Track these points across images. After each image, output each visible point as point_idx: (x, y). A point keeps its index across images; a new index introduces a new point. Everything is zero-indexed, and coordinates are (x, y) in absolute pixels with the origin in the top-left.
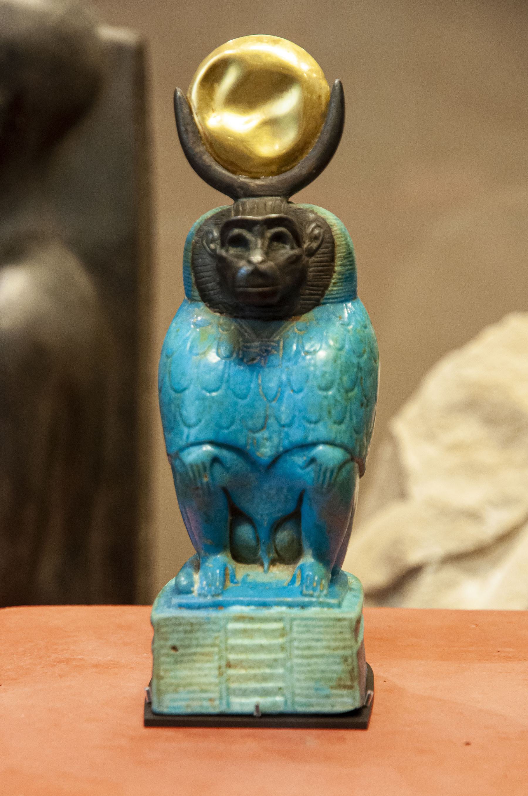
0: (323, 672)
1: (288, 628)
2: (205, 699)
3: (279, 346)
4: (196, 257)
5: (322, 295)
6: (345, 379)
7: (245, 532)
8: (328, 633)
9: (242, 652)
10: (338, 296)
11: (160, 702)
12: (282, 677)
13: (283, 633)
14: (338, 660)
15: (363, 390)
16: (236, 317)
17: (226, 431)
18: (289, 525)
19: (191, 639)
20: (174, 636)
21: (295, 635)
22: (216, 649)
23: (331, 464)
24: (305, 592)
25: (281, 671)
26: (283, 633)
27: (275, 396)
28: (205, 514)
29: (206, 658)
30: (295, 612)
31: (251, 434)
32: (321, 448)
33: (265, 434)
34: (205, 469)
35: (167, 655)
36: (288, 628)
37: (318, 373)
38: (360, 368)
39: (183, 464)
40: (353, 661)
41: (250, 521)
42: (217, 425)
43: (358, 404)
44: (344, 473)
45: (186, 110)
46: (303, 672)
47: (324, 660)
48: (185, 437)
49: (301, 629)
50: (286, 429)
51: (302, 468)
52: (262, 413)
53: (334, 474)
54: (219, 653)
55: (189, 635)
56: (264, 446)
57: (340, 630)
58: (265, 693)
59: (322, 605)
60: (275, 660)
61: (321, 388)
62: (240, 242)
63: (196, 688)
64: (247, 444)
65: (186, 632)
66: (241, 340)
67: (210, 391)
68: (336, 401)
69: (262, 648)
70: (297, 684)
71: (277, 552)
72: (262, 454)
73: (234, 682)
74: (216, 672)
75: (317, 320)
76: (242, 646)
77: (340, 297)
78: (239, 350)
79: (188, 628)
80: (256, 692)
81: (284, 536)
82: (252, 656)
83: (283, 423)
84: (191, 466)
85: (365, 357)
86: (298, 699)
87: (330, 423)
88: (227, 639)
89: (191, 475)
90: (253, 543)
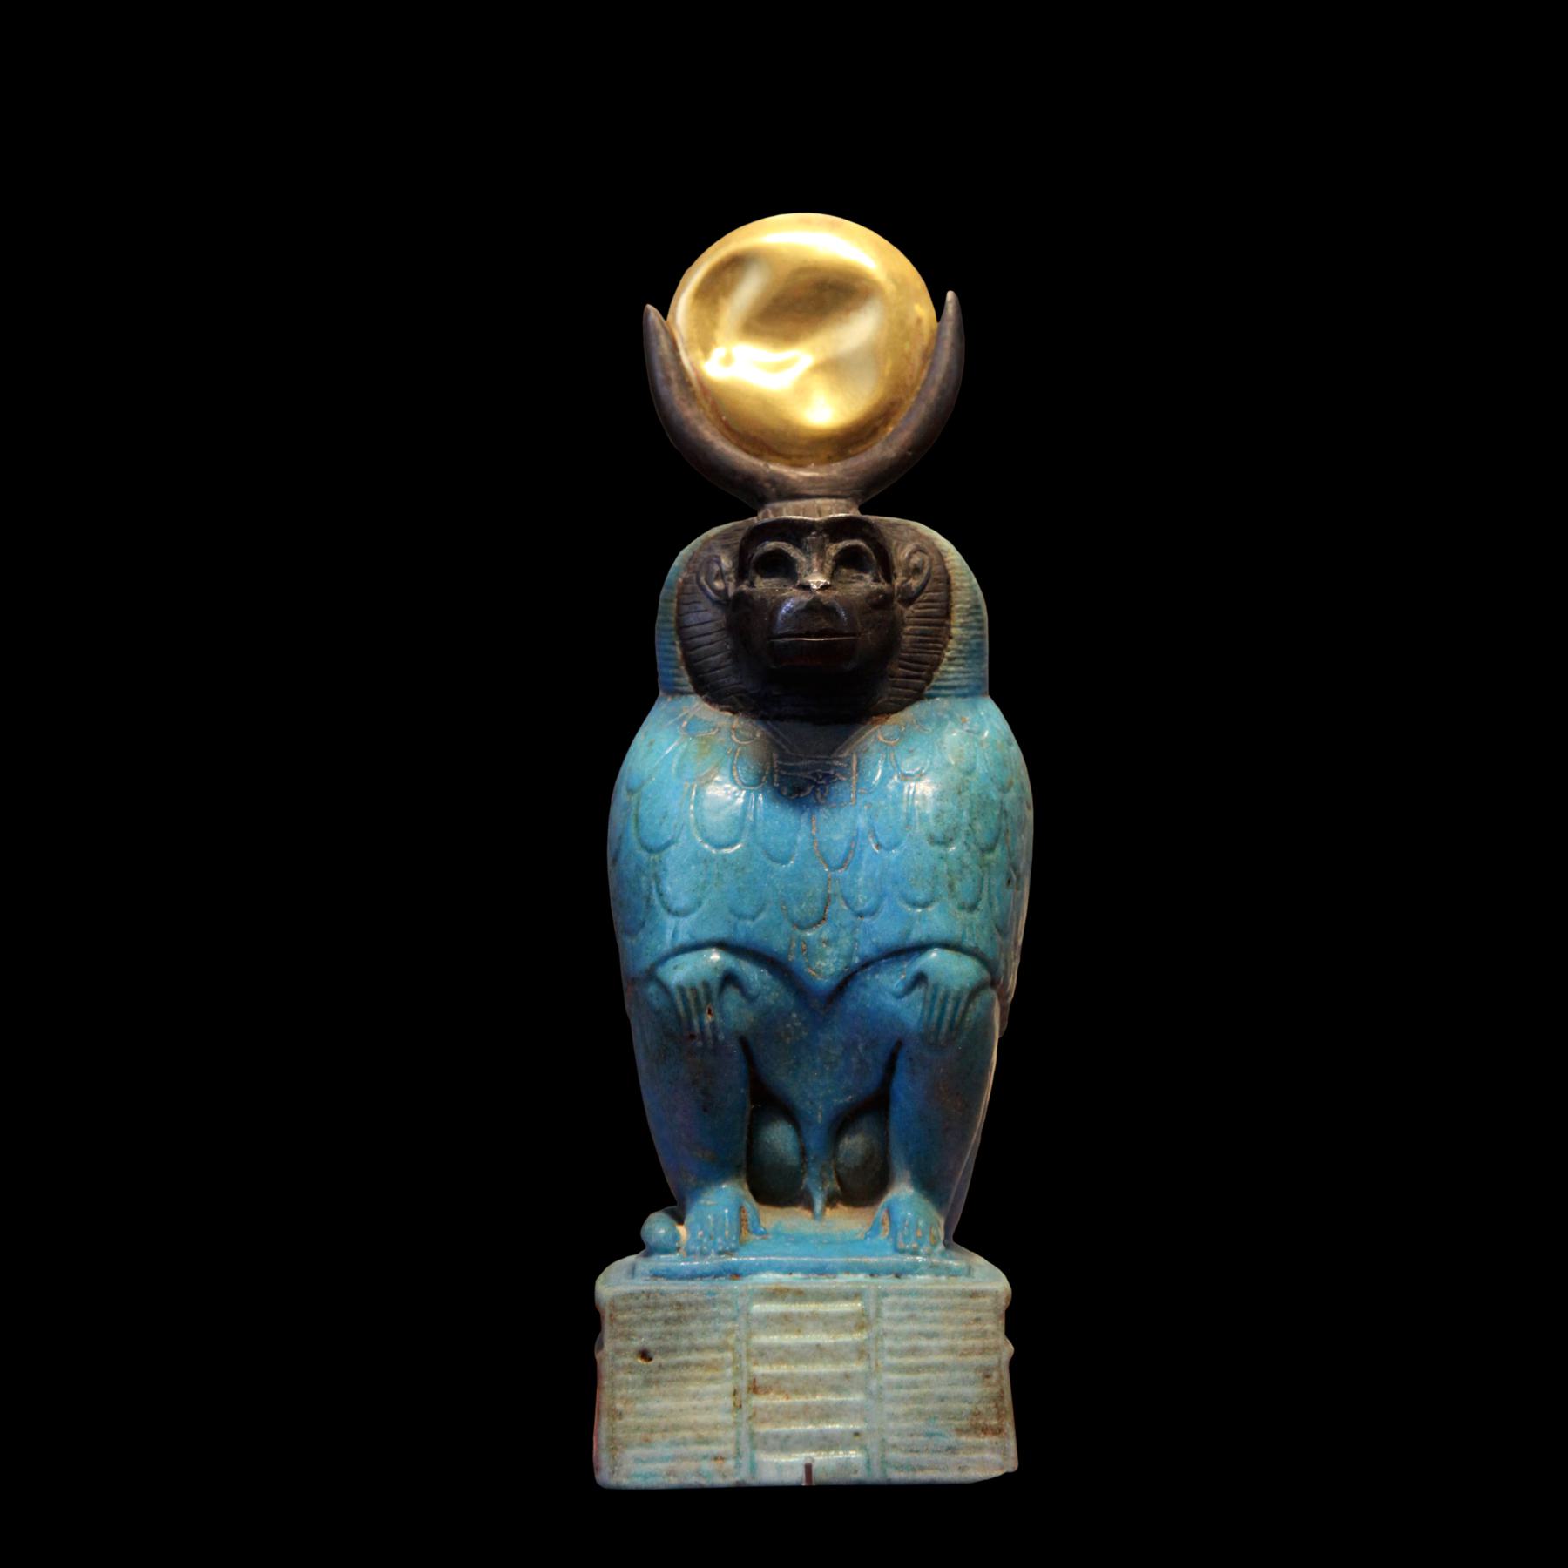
0: (942, 1399)
1: (872, 1311)
2: (705, 1457)
3: (849, 764)
4: (686, 608)
5: (929, 680)
7: (780, 1137)
8: (951, 1322)
9: (781, 1361)
10: (956, 683)
11: (614, 1464)
12: (860, 1411)
13: (861, 1322)
14: (972, 1375)
15: (1010, 855)
16: (763, 718)
17: (749, 923)
18: (865, 1123)
19: (677, 1335)
20: (645, 1329)
21: (887, 1326)
22: (729, 1355)
23: (955, 987)
24: (901, 1245)
25: (857, 1398)
26: (861, 1322)
27: (845, 860)
28: (705, 1092)
29: (709, 1374)
30: (885, 1282)
31: (798, 932)
32: (934, 955)
33: (825, 932)
34: (708, 997)
35: (630, 1369)
36: (872, 1311)
37: (929, 811)
38: (1004, 813)
39: (664, 987)
40: (1001, 1376)
41: (790, 1114)
42: (732, 911)
43: (1002, 878)
44: (977, 1007)
45: (664, 345)
46: (903, 1400)
47: (944, 1376)
48: (668, 937)
49: (898, 1313)
50: (866, 920)
51: (899, 996)
52: (819, 891)
53: (962, 1007)
54: (734, 1362)
55: (674, 1329)
56: (823, 957)
57: (975, 1315)
58: (828, 1443)
59: (934, 1269)
60: (847, 1376)
61: (933, 840)
62: (780, 566)
63: (688, 1434)
64: (789, 951)
65: (667, 1321)
66: (775, 756)
67: (719, 847)
68: (964, 866)
69: (820, 1351)
70: (891, 1425)
71: (840, 1180)
72: (818, 972)
73: (764, 1421)
74: (729, 1402)
75: (920, 721)
76: (781, 1347)
77: (960, 687)
78: (772, 772)
79: (671, 1313)
80: (807, 1442)
81: (854, 1144)
82: (803, 1369)
83: (858, 909)
84: (681, 989)
85: (1012, 794)
86: (893, 1455)
87: (952, 905)
88: (750, 1334)
89: (681, 1009)
90: (793, 1159)
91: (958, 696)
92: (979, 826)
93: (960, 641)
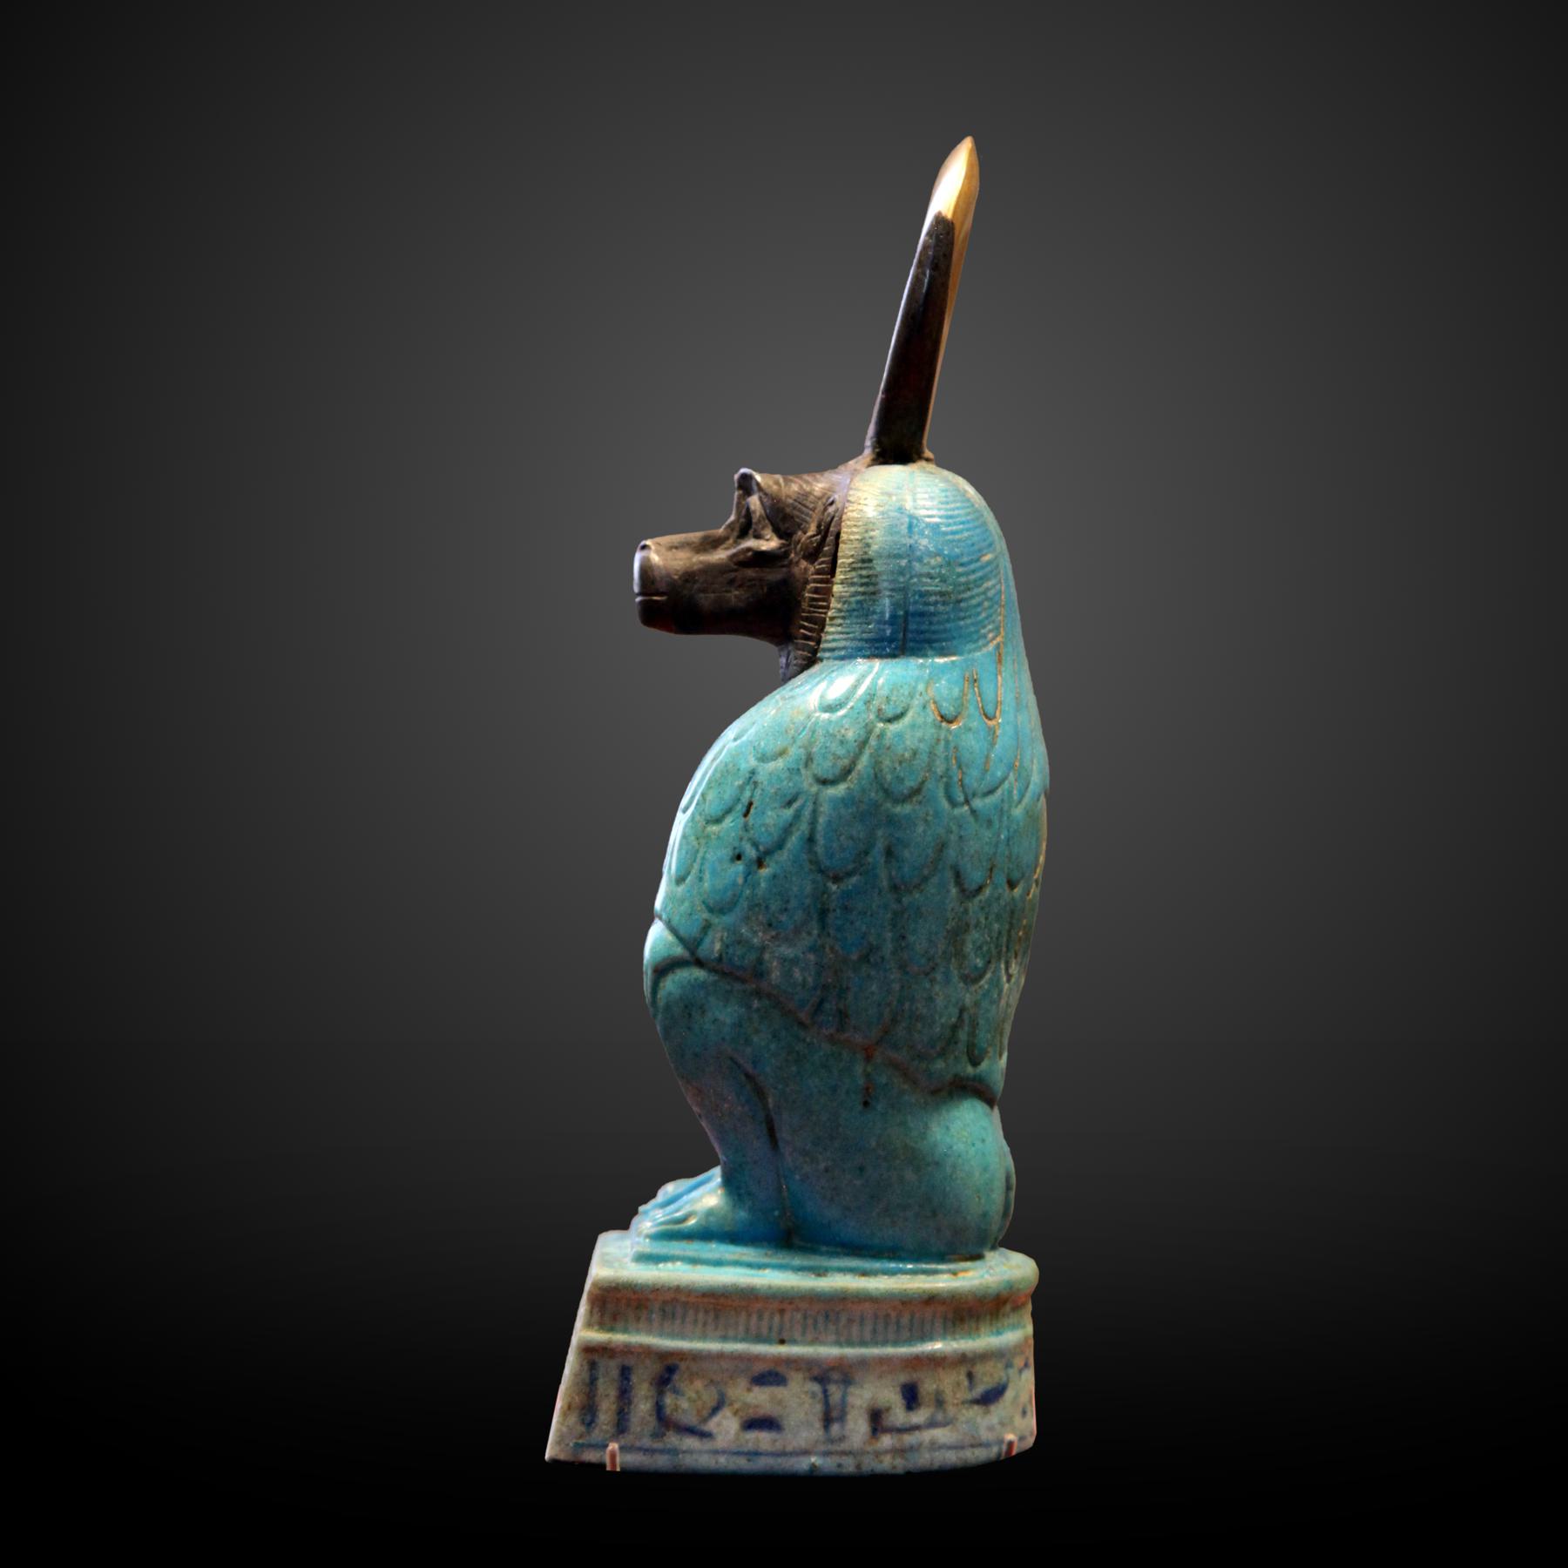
5: (819, 642)
6: (710, 796)
43: (726, 853)
91: (842, 658)
92: (710, 796)
93: (840, 599)
